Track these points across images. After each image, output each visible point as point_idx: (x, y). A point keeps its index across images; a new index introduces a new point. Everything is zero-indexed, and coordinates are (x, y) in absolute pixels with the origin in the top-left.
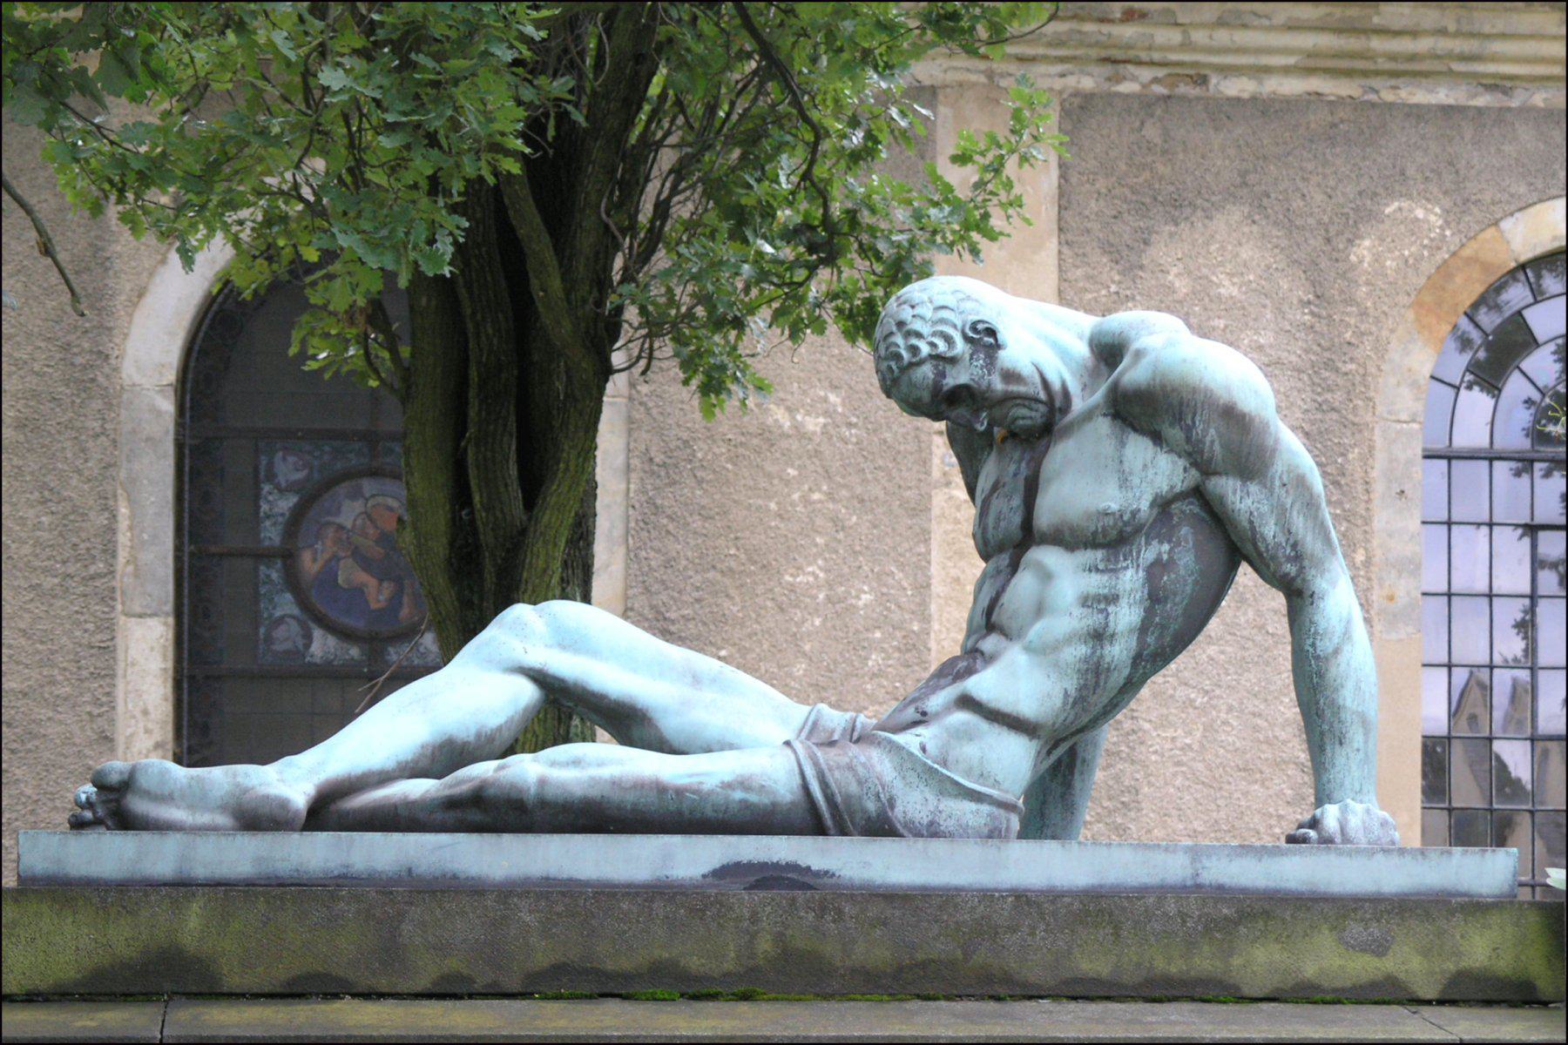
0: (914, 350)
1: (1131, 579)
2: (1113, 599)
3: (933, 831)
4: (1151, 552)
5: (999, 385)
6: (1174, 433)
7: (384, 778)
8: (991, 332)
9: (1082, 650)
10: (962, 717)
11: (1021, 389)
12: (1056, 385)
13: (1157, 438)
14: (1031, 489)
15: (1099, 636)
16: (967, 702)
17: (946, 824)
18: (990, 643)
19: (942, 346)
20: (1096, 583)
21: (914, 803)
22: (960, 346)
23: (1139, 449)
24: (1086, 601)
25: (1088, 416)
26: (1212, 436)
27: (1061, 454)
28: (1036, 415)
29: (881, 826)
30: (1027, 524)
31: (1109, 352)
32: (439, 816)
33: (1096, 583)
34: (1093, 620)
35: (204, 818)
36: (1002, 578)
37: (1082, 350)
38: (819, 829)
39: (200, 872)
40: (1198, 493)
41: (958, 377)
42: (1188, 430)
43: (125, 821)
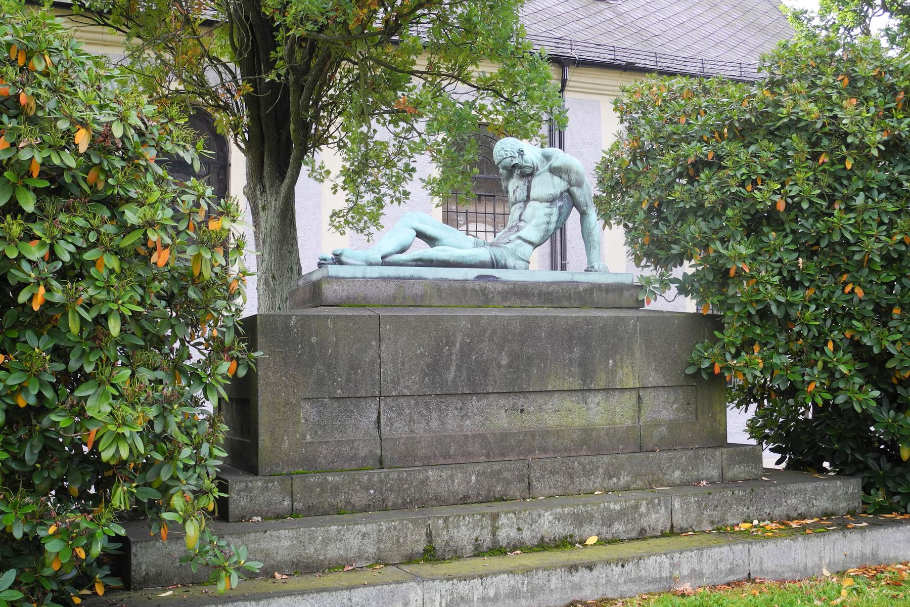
0: (506, 154)
1: (555, 210)
2: (551, 214)
3: (515, 268)
4: (560, 204)
5: (524, 164)
6: (565, 176)
7: (391, 254)
8: (522, 151)
9: (545, 226)
10: (519, 241)
11: (528, 165)
12: (535, 165)
13: (561, 177)
14: (529, 189)
15: (548, 223)
16: (520, 238)
17: (517, 267)
18: (522, 224)
19: (512, 155)
20: (548, 211)
21: (511, 262)
22: (517, 155)
23: (557, 179)
24: (545, 215)
25: (544, 172)
26: (573, 178)
27: (535, 181)
28: (528, 171)
29: (505, 267)
30: (528, 197)
31: (547, 158)
32: (410, 263)
33: (548, 211)
34: (547, 219)
35: (359, 263)
36: (522, 209)
37: (540, 156)
38: (493, 267)
39: (368, 276)
40: (568, 191)
41: (515, 161)
42: (569, 176)
43: (341, 263)
